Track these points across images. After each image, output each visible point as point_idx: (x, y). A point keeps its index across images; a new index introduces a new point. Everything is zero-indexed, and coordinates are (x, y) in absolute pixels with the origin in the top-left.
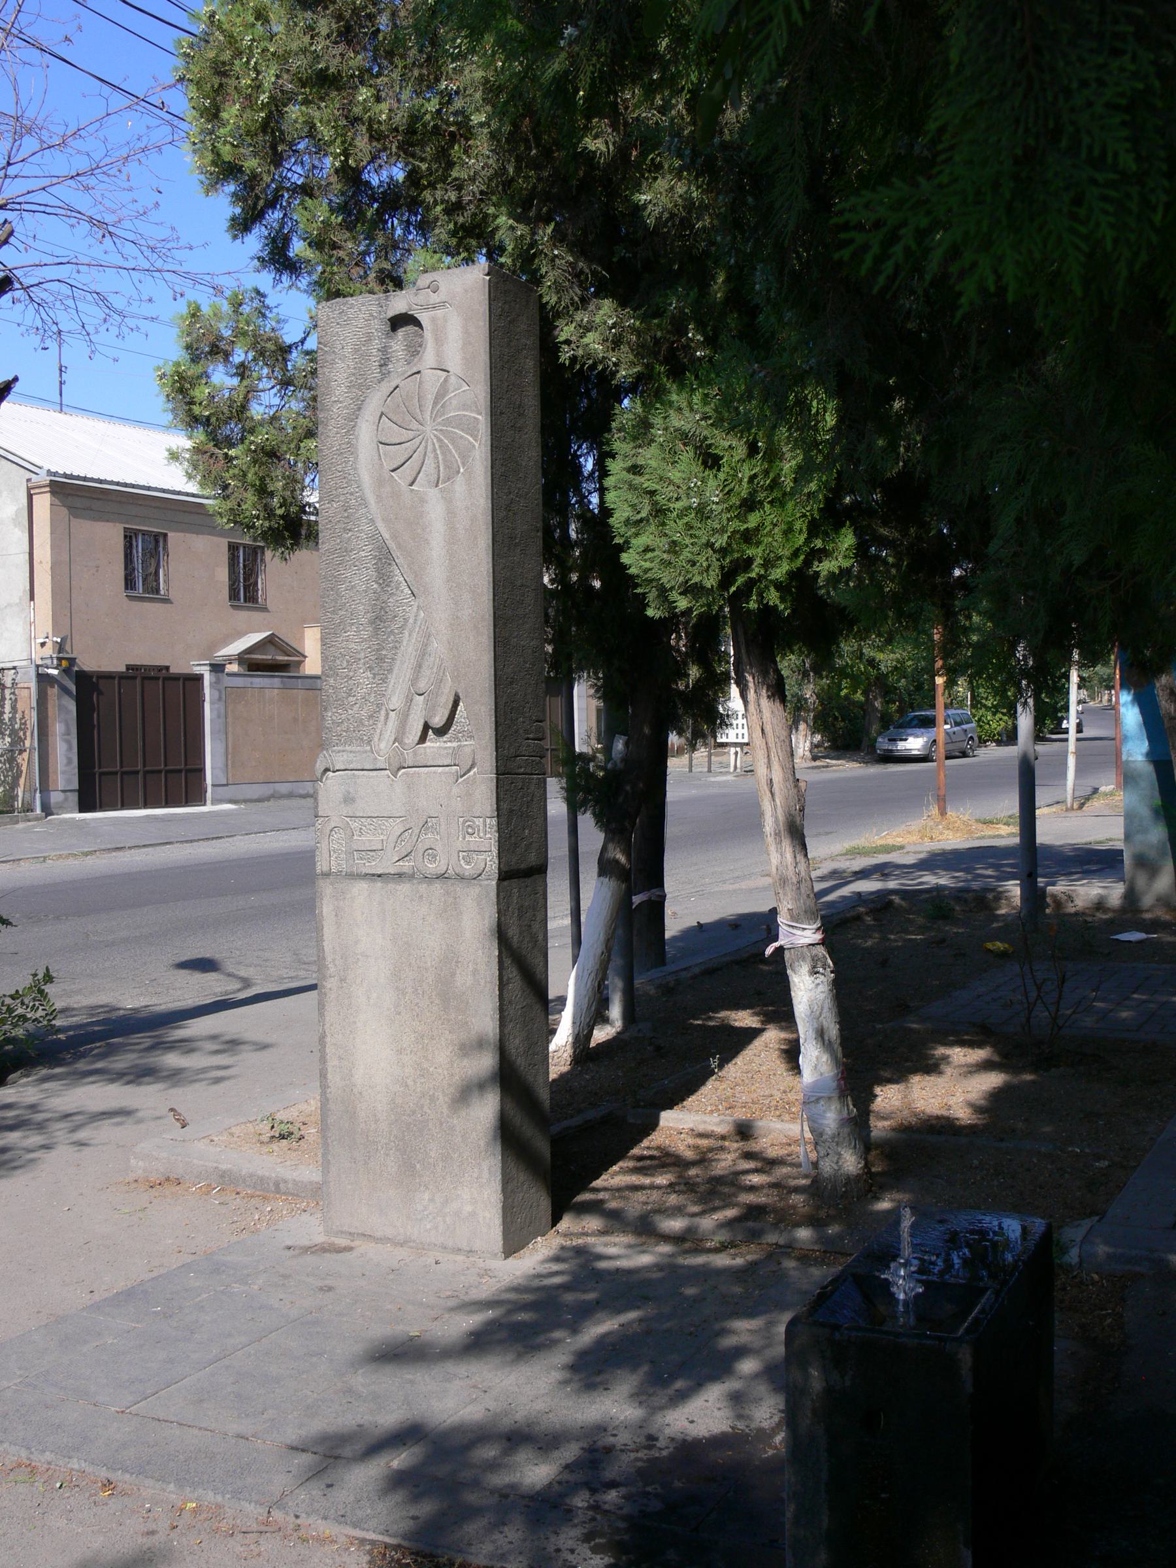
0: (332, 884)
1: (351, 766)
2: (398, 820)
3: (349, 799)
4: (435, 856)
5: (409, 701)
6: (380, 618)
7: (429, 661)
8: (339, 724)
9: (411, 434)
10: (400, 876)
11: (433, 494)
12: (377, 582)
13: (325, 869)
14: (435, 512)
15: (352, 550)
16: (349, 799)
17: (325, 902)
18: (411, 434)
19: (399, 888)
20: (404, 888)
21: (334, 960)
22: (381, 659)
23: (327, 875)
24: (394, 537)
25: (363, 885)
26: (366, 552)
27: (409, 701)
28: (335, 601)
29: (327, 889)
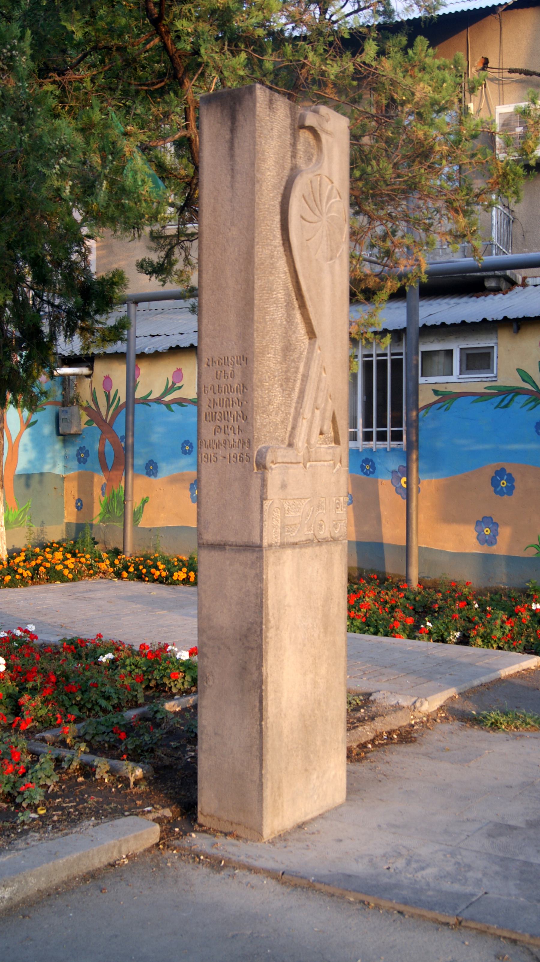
0: (274, 553)
1: (285, 460)
2: (307, 501)
3: (284, 486)
4: (321, 525)
5: (313, 413)
6: (288, 349)
7: (322, 385)
8: (265, 426)
9: (315, 218)
10: (308, 543)
11: (326, 266)
12: (286, 320)
13: (269, 542)
14: (327, 280)
15: (274, 291)
16: (284, 486)
17: (269, 568)
18: (315, 218)
19: (307, 551)
20: (309, 551)
21: (273, 614)
22: (287, 379)
23: (270, 546)
24: (309, 290)
25: (289, 552)
26: (281, 296)
27: (313, 413)
28: (264, 327)
29: (270, 557)
